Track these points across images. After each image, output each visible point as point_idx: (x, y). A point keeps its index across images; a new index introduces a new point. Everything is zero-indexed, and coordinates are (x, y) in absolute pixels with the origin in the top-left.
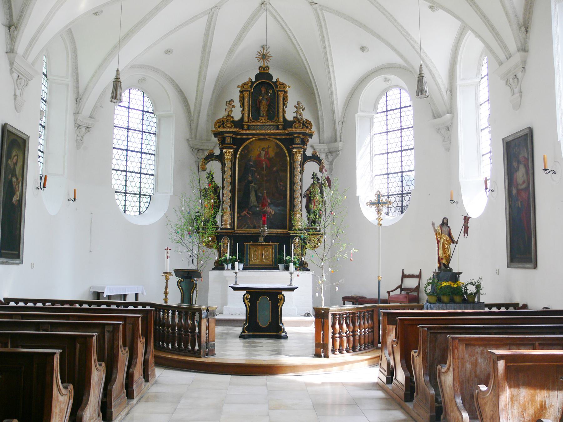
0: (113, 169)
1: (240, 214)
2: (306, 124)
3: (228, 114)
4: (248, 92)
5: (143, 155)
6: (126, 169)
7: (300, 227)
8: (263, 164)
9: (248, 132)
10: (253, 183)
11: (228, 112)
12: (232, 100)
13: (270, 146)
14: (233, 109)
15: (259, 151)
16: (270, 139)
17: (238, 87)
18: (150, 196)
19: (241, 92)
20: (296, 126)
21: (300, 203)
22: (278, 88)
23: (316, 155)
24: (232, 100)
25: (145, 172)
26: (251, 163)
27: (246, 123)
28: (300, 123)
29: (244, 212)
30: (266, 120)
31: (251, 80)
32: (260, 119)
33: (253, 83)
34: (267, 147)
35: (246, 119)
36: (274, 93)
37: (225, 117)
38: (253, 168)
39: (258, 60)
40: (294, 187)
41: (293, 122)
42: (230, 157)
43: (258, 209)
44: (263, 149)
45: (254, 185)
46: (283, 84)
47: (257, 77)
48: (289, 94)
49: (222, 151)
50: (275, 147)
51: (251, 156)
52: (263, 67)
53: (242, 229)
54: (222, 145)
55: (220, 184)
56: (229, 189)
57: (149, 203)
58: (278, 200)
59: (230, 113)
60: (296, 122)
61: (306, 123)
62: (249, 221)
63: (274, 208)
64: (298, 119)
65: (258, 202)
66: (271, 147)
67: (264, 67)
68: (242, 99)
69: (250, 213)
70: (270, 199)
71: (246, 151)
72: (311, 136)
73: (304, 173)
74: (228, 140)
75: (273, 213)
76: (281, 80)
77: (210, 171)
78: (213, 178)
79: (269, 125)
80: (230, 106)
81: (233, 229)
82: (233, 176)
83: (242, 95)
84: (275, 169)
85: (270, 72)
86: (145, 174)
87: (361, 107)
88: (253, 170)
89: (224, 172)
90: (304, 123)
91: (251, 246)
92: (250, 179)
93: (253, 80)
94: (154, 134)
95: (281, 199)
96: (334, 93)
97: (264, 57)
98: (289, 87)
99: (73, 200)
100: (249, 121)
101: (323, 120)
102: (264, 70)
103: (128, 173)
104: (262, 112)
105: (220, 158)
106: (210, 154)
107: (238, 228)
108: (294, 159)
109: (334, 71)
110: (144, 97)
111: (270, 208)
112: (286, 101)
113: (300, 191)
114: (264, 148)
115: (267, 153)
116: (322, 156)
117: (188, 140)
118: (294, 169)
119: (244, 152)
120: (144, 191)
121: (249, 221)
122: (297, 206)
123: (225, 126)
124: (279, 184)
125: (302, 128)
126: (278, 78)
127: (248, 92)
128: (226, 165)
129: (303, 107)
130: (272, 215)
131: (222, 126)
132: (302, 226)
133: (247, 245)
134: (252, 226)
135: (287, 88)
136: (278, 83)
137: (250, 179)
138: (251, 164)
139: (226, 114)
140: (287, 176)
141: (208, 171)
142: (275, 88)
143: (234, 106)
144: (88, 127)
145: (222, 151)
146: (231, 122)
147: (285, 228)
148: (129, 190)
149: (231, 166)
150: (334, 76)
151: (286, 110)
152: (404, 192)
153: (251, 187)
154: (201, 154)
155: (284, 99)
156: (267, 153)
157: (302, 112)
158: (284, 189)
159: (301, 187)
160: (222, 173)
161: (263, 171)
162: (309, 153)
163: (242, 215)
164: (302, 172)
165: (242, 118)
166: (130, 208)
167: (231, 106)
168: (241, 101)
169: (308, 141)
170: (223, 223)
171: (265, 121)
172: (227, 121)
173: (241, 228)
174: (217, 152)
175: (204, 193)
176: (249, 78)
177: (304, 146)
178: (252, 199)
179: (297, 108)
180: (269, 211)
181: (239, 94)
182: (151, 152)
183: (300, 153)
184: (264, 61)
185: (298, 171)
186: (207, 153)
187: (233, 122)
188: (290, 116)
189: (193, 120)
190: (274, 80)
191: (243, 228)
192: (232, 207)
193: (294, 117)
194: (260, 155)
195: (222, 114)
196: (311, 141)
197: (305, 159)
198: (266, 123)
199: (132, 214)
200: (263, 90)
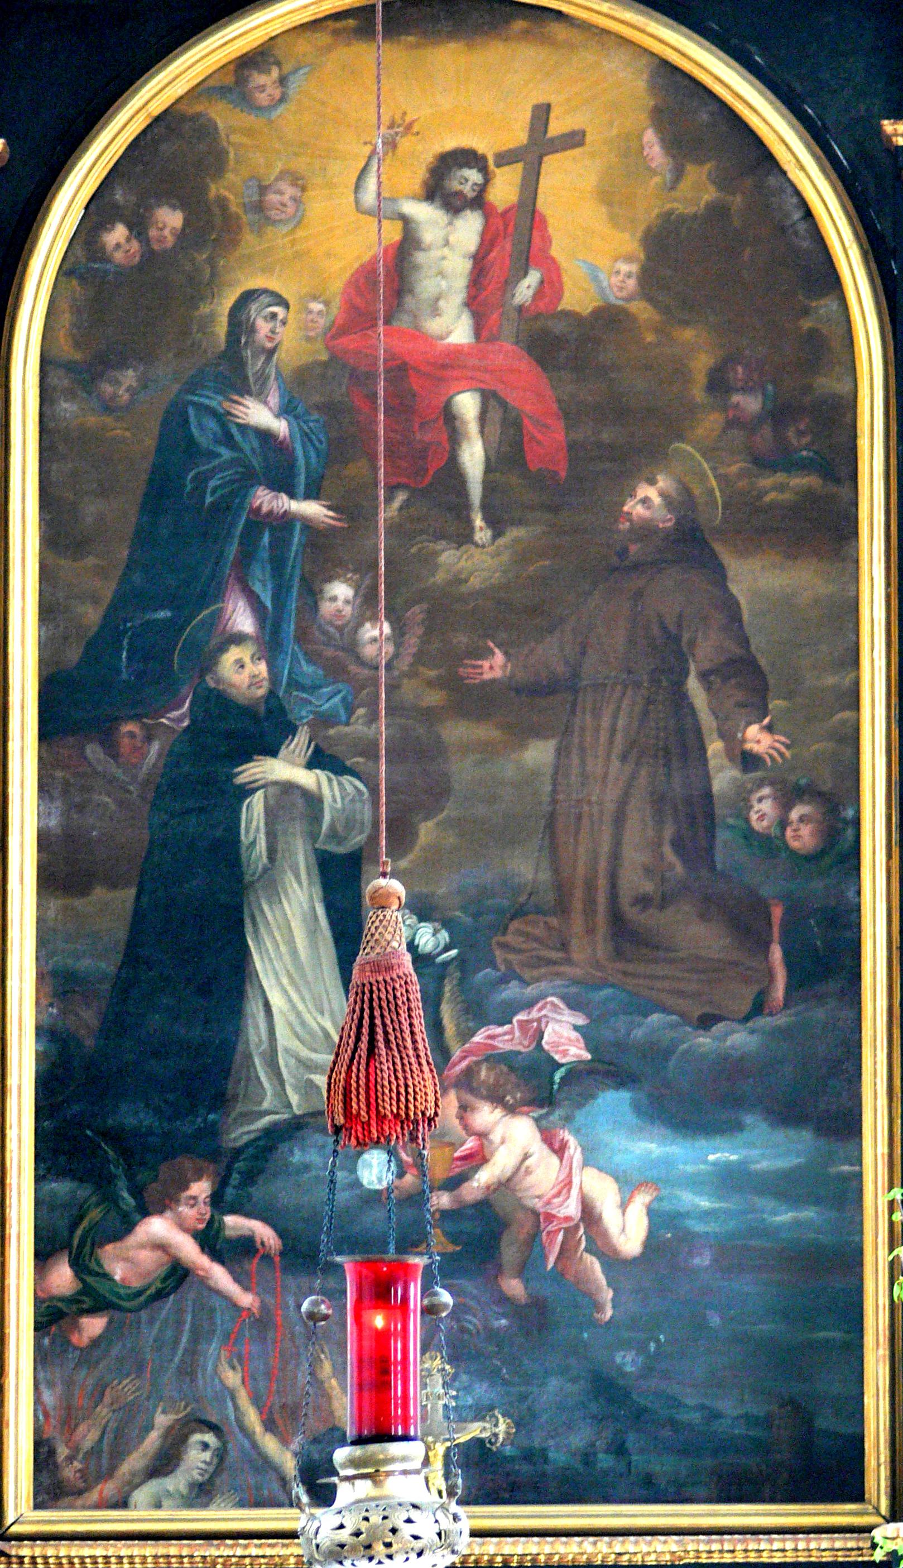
1: (78, 1265)
8: (450, 417)
10: (300, 743)
13: (556, 127)
15: (377, 213)
34: (518, 136)
38: (287, 487)
45: (307, 778)
50: (652, 142)
51: (248, 297)
53: (123, 1504)
58: (706, 1022)
62: (232, 1378)
66: (574, 140)
69: (247, 1246)
70: (574, 1004)
88: (286, 521)
95: (759, 1007)
111: (574, 1150)
119: (138, 227)
121: (232, 1378)
124: (715, 747)
134: (290, 1465)
138: (265, 436)
153: (257, 803)
161: (464, 537)
163: (118, 1272)
173: (109, 1488)
178: (276, 999)
180: (572, 1208)
191: (141, 1495)
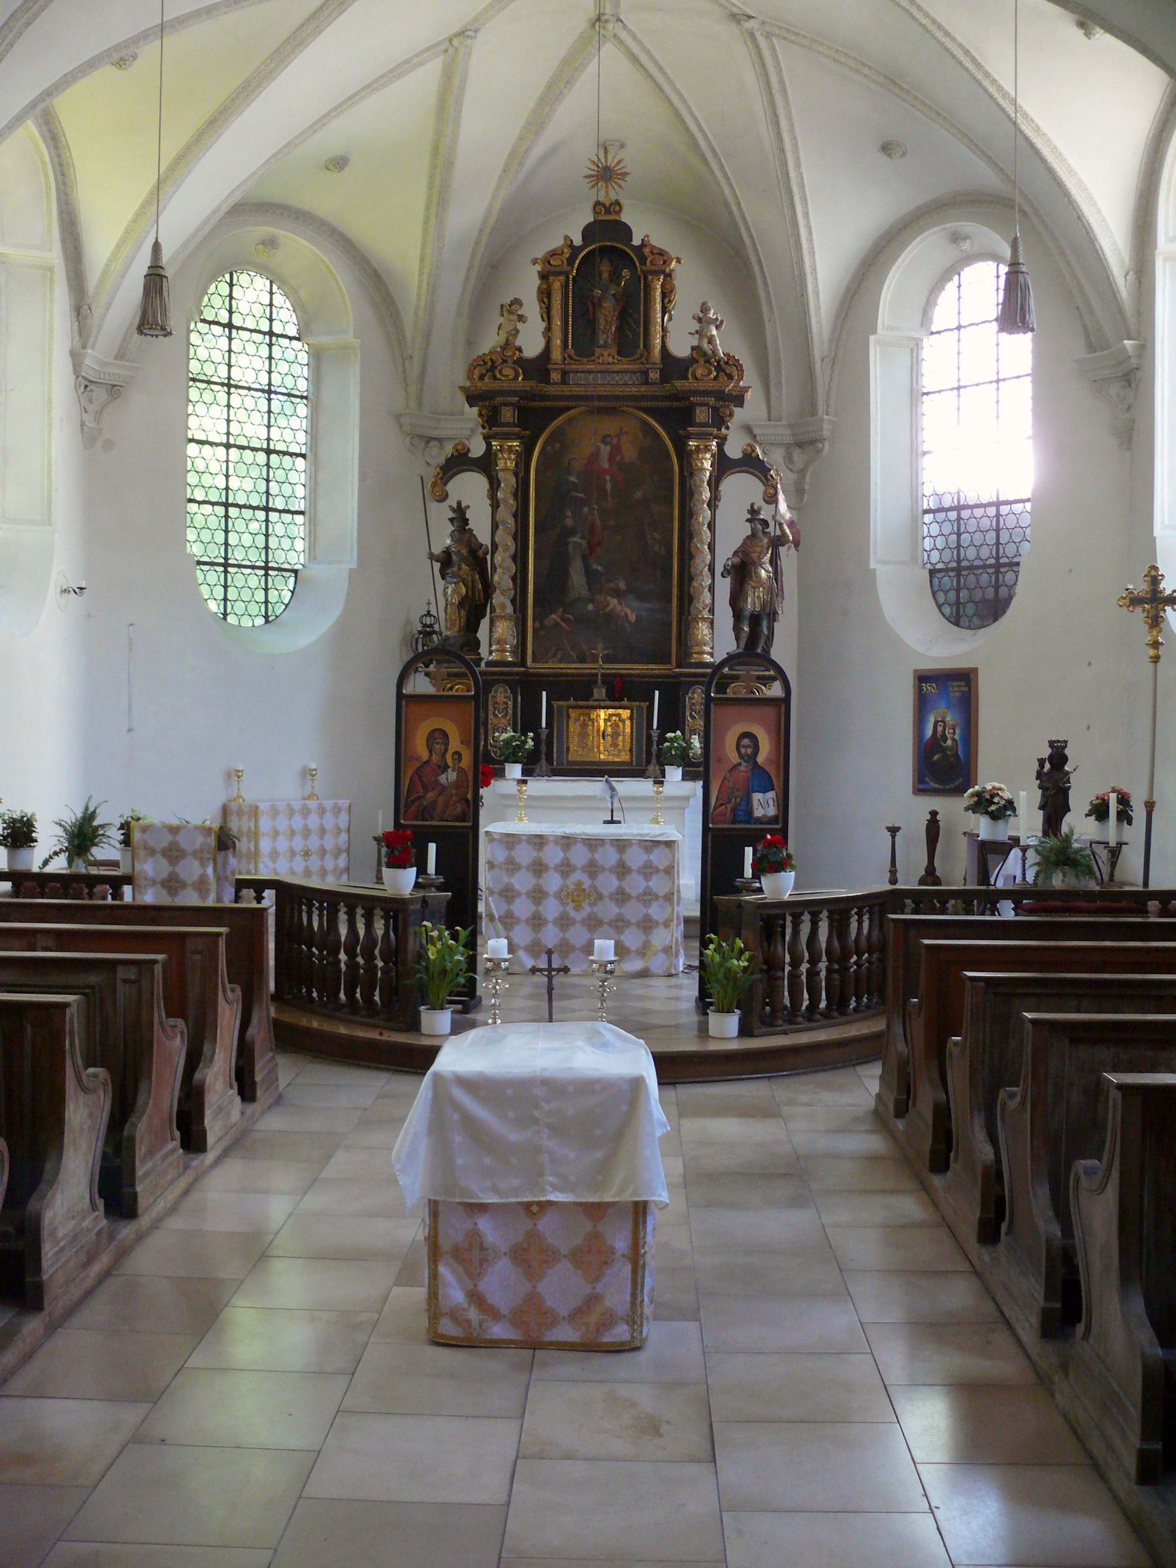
0: (191, 501)
2: (727, 367)
3: (507, 340)
4: (562, 278)
5: (273, 457)
6: (227, 498)
7: (707, 658)
9: (565, 390)
11: (506, 335)
12: (516, 299)
14: (520, 326)
16: (626, 409)
17: (535, 262)
18: (296, 572)
19: (544, 276)
20: (699, 372)
21: (709, 590)
22: (648, 264)
23: (753, 455)
24: (517, 302)
25: (279, 504)
26: (573, 479)
27: (557, 366)
28: (710, 364)
29: (554, 616)
30: (613, 358)
31: (572, 241)
32: (597, 354)
33: (575, 250)
35: (556, 355)
36: (635, 279)
37: (499, 349)
38: (578, 492)
39: (590, 185)
40: (692, 545)
41: (691, 361)
42: (511, 465)
43: (590, 607)
44: (604, 441)
46: (662, 253)
47: (588, 232)
48: (679, 282)
49: (489, 445)
50: (640, 435)
52: (604, 205)
53: (547, 662)
54: (490, 429)
55: (483, 535)
56: (512, 549)
57: (293, 592)
59: (510, 338)
60: (697, 361)
61: (726, 363)
63: (636, 604)
64: (705, 354)
65: (590, 590)
66: (627, 433)
67: (608, 205)
68: (545, 295)
71: (558, 445)
72: (739, 400)
73: (721, 505)
74: (508, 414)
75: (632, 618)
76: (656, 241)
77: (459, 503)
78: (466, 521)
79: (622, 372)
80: (512, 317)
81: (523, 663)
82: (521, 515)
83: (545, 286)
84: (638, 494)
85: (625, 218)
86: (280, 511)
87: (884, 315)
89: (495, 505)
90: (722, 363)
91: (570, 710)
92: (569, 522)
93: (578, 241)
94: (302, 397)
96: (809, 276)
97: (605, 174)
98: (679, 261)
99: (77, 590)
100: (565, 359)
101: (777, 351)
102: (608, 212)
103: (231, 509)
104: (604, 333)
105: (486, 464)
106: (456, 454)
107: (534, 661)
108: (691, 465)
109: (806, 215)
110: (271, 293)
112: (670, 301)
113: (709, 557)
114: (609, 436)
115: (616, 451)
116: (774, 458)
117: (398, 417)
118: (692, 494)
120: (278, 558)
122: (699, 598)
123: (498, 376)
124: (649, 537)
125: (716, 378)
126: (647, 236)
127: (562, 278)
128: (502, 485)
129: (717, 319)
130: (629, 622)
131: (489, 374)
132: (711, 655)
133: (559, 707)
134: (575, 655)
135: (674, 263)
136: (647, 251)
137: (569, 522)
139: (501, 339)
140: (672, 513)
141: (452, 501)
142: (637, 264)
143: (521, 318)
144: (115, 386)
145: (489, 445)
146: (515, 362)
147: (664, 658)
148: (237, 556)
149: (517, 489)
150: (809, 228)
151: (670, 327)
152: (1002, 561)
153: (571, 544)
154: (435, 451)
155: (664, 295)
156: (616, 451)
157: (714, 332)
158: (663, 552)
159: (712, 547)
160: (492, 506)
162: (734, 450)
164: (713, 504)
165: (547, 352)
166: (239, 607)
167: (516, 317)
168: (544, 303)
169: (731, 415)
170: (494, 647)
171: (610, 360)
172: (504, 361)
174: (477, 448)
175: (446, 561)
176: (566, 238)
177: (720, 429)
179: (700, 320)
180: (623, 614)
181: (536, 282)
182: (294, 449)
183: (709, 450)
184: (607, 187)
185: (703, 501)
186: (449, 449)
187: (522, 363)
188: (680, 347)
189: (411, 357)
190: (636, 242)
192: (519, 602)
193: (693, 348)
194: (595, 455)
195: (490, 341)
196: (740, 415)
197: (723, 465)
198: (613, 363)
199: (246, 622)
200: (605, 269)
